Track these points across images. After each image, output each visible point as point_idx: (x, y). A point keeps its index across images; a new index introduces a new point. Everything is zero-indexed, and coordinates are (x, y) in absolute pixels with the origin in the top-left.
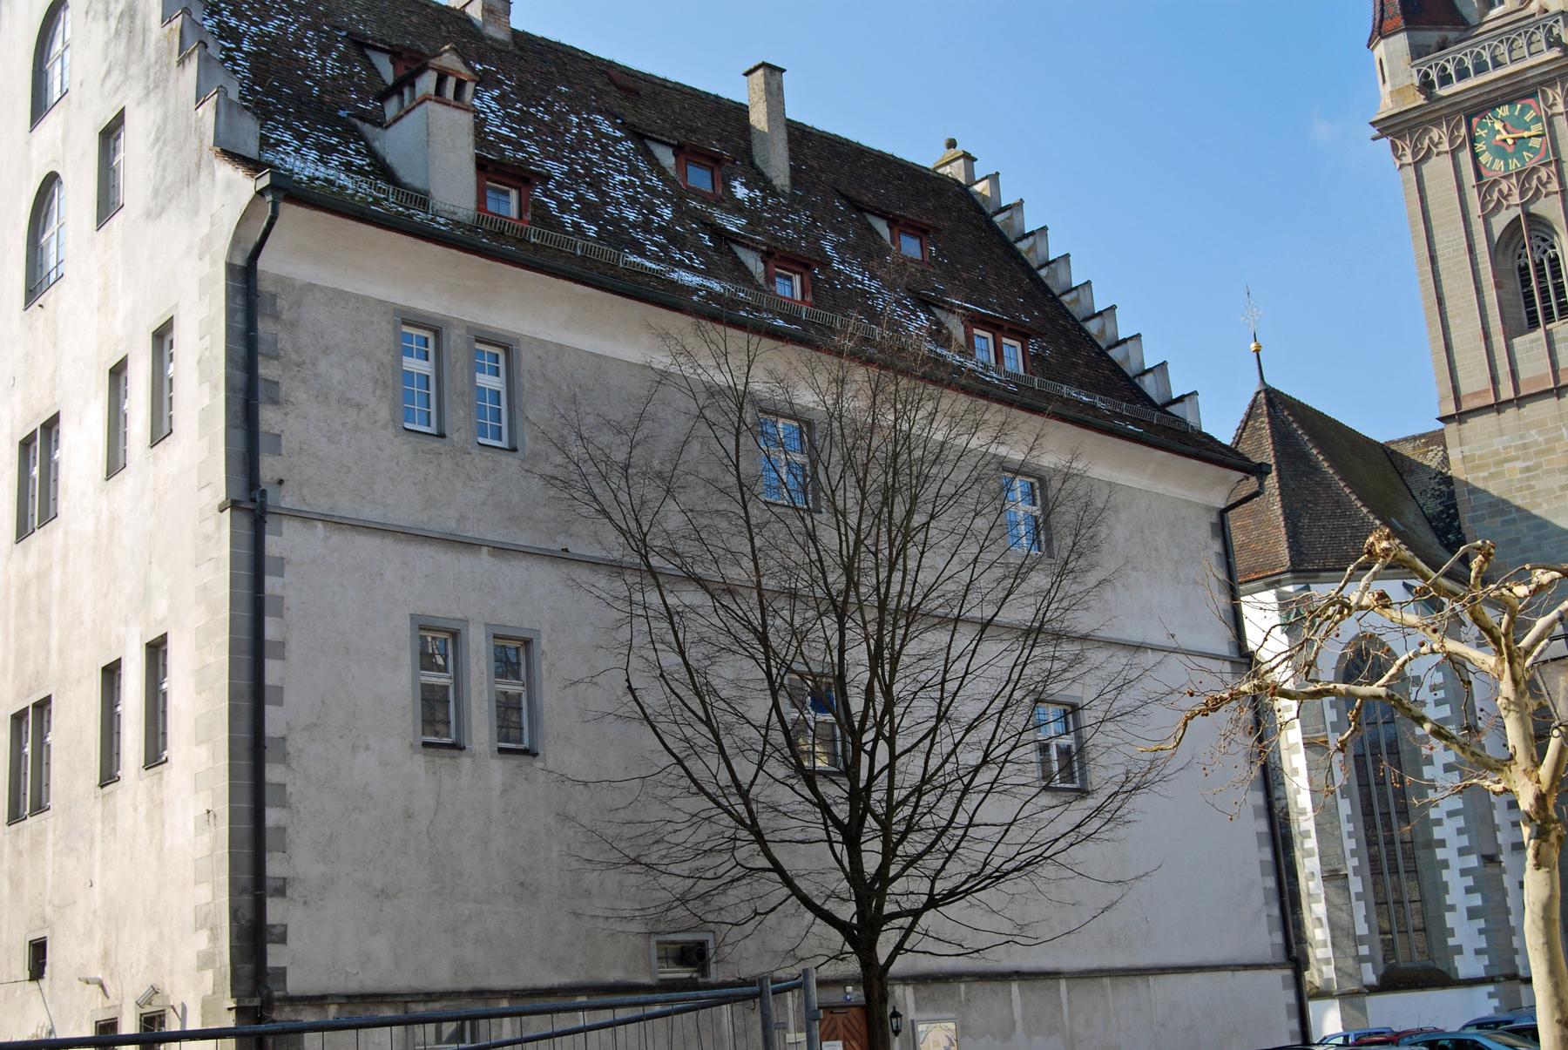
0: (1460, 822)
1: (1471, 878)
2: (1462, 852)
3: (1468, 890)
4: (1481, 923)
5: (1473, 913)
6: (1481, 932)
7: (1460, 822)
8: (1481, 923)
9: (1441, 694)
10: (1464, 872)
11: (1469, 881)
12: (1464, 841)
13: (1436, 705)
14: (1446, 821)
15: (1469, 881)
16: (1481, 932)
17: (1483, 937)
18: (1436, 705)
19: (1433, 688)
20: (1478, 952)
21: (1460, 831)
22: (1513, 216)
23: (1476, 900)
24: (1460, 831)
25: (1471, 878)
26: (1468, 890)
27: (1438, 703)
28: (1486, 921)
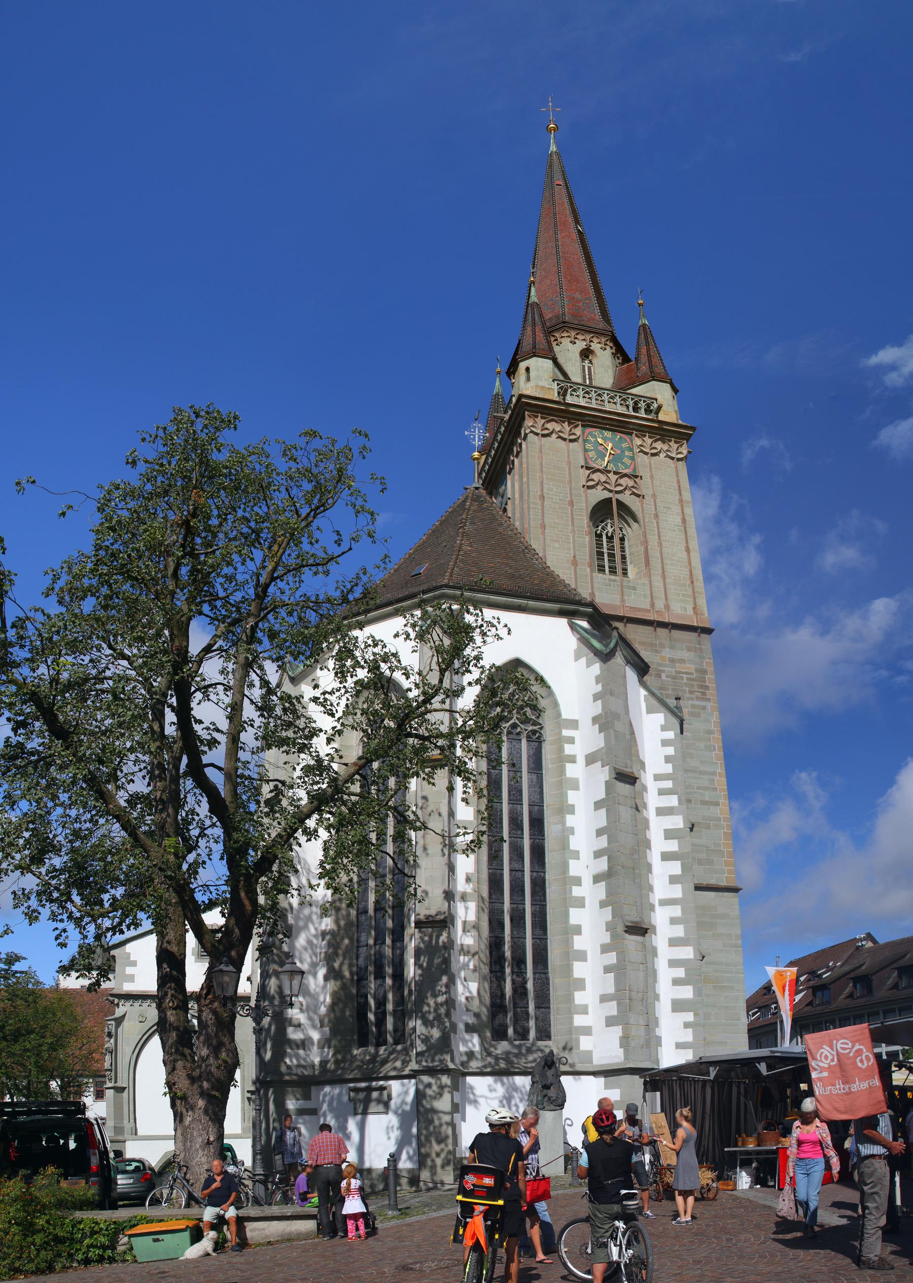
0: (677, 911)
1: (683, 969)
2: (674, 942)
3: (676, 982)
4: (690, 1017)
5: (678, 1006)
6: (687, 1025)
7: (677, 911)
8: (690, 1017)
9: (669, 784)
10: (673, 963)
11: (680, 973)
12: (679, 931)
13: (660, 794)
14: (658, 908)
15: (680, 973)
16: (687, 1025)
17: (690, 1031)
18: (660, 794)
19: (657, 777)
20: (679, 1046)
21: (674, 921)
22: (607, 496)
23: (687, 993)
24: (674, 921)
25: (683, 969)
26: (676, 982)
27: (662, 792)
28: (695, 1015)
